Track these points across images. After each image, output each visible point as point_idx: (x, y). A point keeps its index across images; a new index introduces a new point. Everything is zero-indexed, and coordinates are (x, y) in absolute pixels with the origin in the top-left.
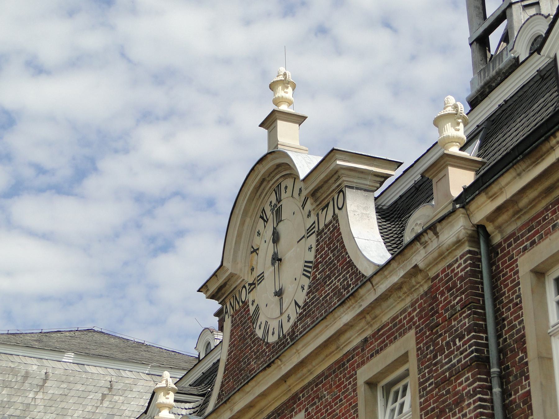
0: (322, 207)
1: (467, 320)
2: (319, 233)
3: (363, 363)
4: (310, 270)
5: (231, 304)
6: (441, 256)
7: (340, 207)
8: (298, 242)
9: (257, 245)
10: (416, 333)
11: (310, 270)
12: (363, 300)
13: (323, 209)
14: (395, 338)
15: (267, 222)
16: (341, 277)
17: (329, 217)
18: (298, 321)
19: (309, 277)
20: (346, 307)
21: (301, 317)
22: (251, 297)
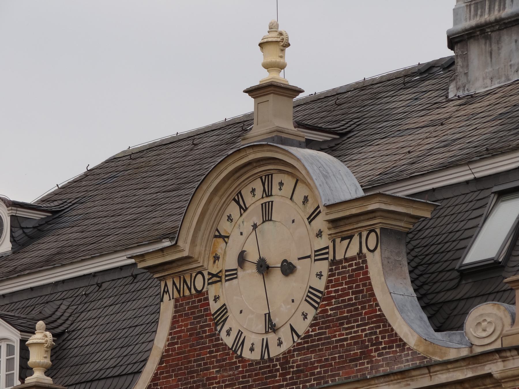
0: (343, 236)
2: (334, 262)
5: (174, 283)
7: (372, 248)
8: (299, 259)
9: (226, 232)
12: (412, 380)
13: (343, 239)
15: (245, 211)
16: (367, 327)
17: (353, 251)
18: (294, 350)
19: (316, 308)
20: (387, 379)
21: (298, 348)
22: (212, 291)
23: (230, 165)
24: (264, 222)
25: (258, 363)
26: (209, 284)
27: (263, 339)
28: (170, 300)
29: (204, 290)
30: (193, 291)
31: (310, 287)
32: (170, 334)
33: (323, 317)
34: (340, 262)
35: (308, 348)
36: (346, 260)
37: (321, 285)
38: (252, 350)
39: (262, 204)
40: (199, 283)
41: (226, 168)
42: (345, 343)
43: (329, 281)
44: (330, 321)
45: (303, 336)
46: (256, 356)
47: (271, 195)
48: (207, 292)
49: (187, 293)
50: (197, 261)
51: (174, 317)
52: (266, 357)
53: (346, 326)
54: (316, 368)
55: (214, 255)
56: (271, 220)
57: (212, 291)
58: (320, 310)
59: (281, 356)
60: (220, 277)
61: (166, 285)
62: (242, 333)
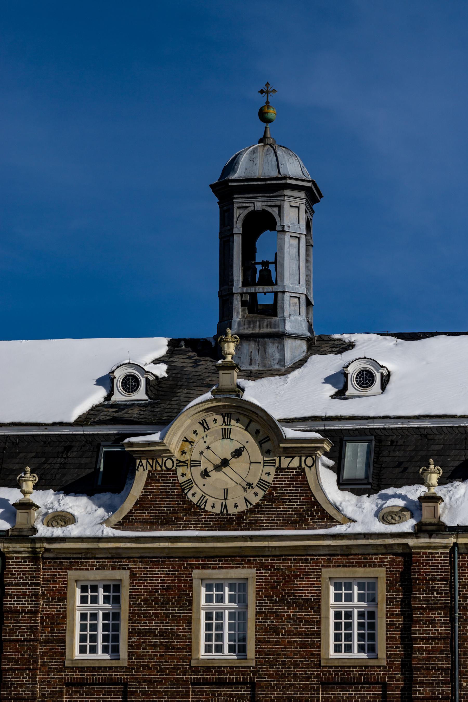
1: (443, 586)
2: (279, 468)
3: (329, 567)
4: (267, 487)
5: (148, 461)
6: (429, 547)
10: (387, 571)
11: (267, 487)
13: (286, 457)
14: (365, 566)
15: (207, 430)
16: (304, 506)
18: (247, 512)
19: (265, 491)
22: (180, 471)
24: (223, 438)
25: (219, 514)
27: (222, 502)
28: (144, 470)
29: (174, 468)
30: (164, 468)
32: (144, 489)
33: (270, 496)
34: (284, 469)
35: (258, 512)
36: (288, 468)
37: (270, 479)
38: (213, 506)
39: (222, 429)
40: (169, 464)
42: (288, 513)
43: (274, 478)
44: (275, 499)
45: (254, 505)
46: (217, 510)
47: (230, 425)
48: (176, 471)
49: (159, 468)
51: (147, 480)
52: (225, 512)
54: (266, 523)
55: (182, 450)
56: (229, 438)
57: (180, 471)
58: (266, 493)
60: (187, 464)
61: (141, 461)
62: (205, 497)
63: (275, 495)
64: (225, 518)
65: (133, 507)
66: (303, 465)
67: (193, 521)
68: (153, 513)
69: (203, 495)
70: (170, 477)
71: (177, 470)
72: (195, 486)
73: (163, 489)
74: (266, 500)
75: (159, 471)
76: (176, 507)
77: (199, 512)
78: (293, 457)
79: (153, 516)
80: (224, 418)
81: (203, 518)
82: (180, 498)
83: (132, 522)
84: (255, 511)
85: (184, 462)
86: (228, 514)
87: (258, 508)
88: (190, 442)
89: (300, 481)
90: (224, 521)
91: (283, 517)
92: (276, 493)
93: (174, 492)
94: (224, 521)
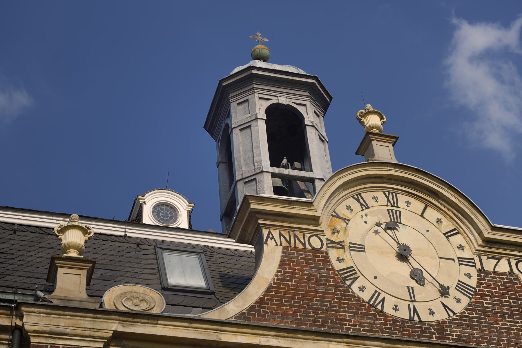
0: (490, 256)
2: (481, 271)
5: (281, 234)
9: (346, 216)
15: (367, 208)
18: (450, 323)
19: (471, 298)
23: (368, 170)
26: (328, 247)
28: (277, 245)
29: (324, 249)
30: (307, 246)
31: (459, 281)
32: (278, 271)
33: (479, 306)
34: (489, 273)
36: (495, 273)
40: (316, 243)
41: (362, 171)
43: (478, 283)
45: (458, 314)
48: (326, 253)
49: (300, 246)
50: (320, 225)
51: (282, 260)
52: (416, 319)
53: (507, 319)
55: (332, 228)
57: (333, 254)
58: (473, 300)
59: (433, 323)
62: (379, 294)
63: (485, 305)
64: (417, 327)
65: (264, 295)
66: (516, 271)
67: (368, 327)
68: (299, 307)
69: (376, 291)
70: (319, 261)
71: (329, 253)
72: (361, 277)
73: (311, 275)
74: (475, 310)
75: (301, 250)
76: (336, 302)
77: (374, 315)
78: (499, 260)
79: (300, 311)
80: (388, 198)
81: (382, 324)
82: (340, 290)
83: (264, 316)
84: (462, 324)
85: (338, 243)
86: (420, 321)
87: (466, 321)
88: (344, 220)
89: (516, 291)
90: (417, 332)
91: (506, 337)
92: (486, 303)
93: (329, 281)
94: (417, 332)
